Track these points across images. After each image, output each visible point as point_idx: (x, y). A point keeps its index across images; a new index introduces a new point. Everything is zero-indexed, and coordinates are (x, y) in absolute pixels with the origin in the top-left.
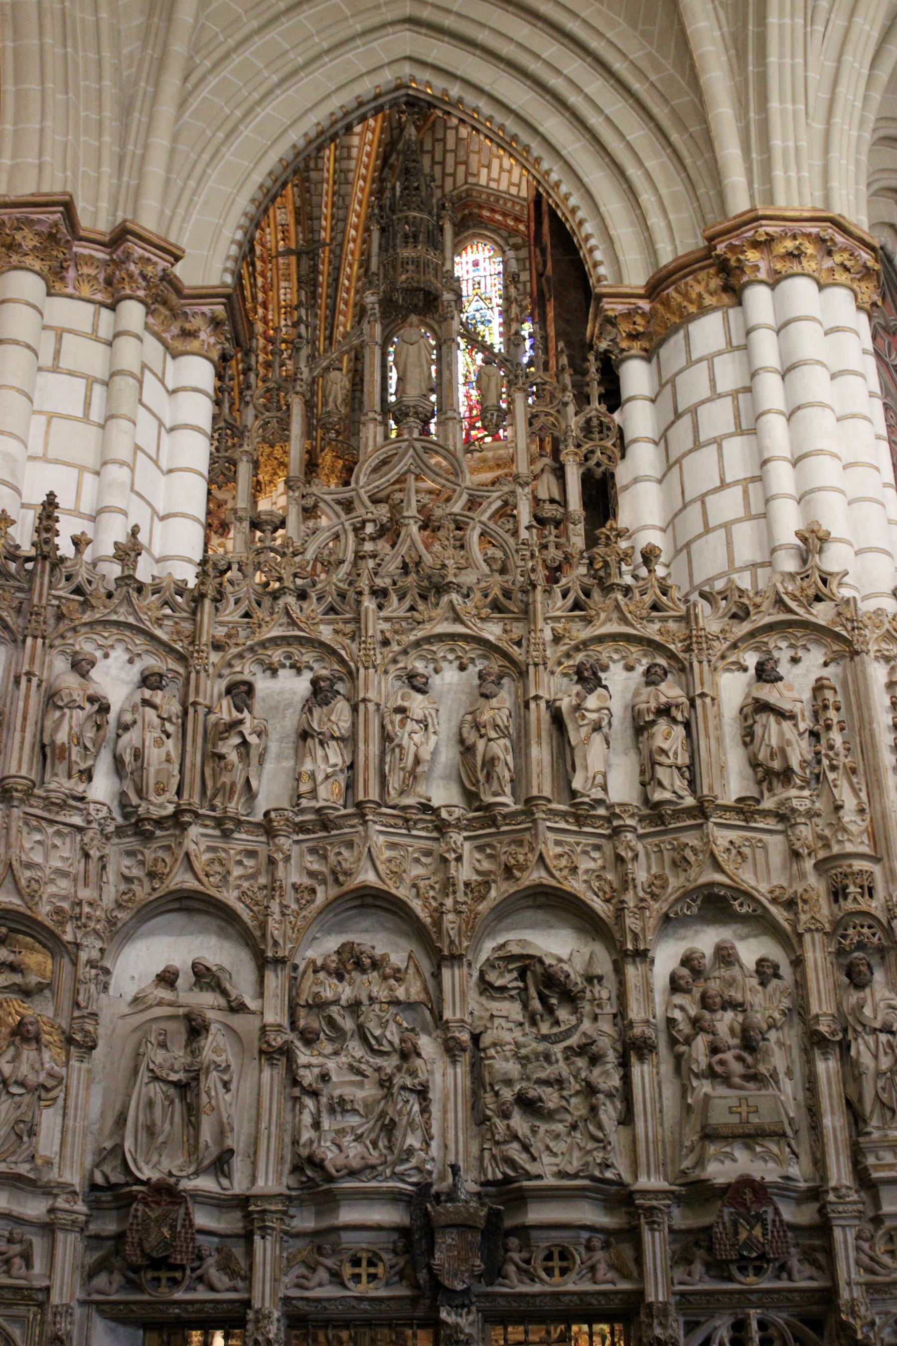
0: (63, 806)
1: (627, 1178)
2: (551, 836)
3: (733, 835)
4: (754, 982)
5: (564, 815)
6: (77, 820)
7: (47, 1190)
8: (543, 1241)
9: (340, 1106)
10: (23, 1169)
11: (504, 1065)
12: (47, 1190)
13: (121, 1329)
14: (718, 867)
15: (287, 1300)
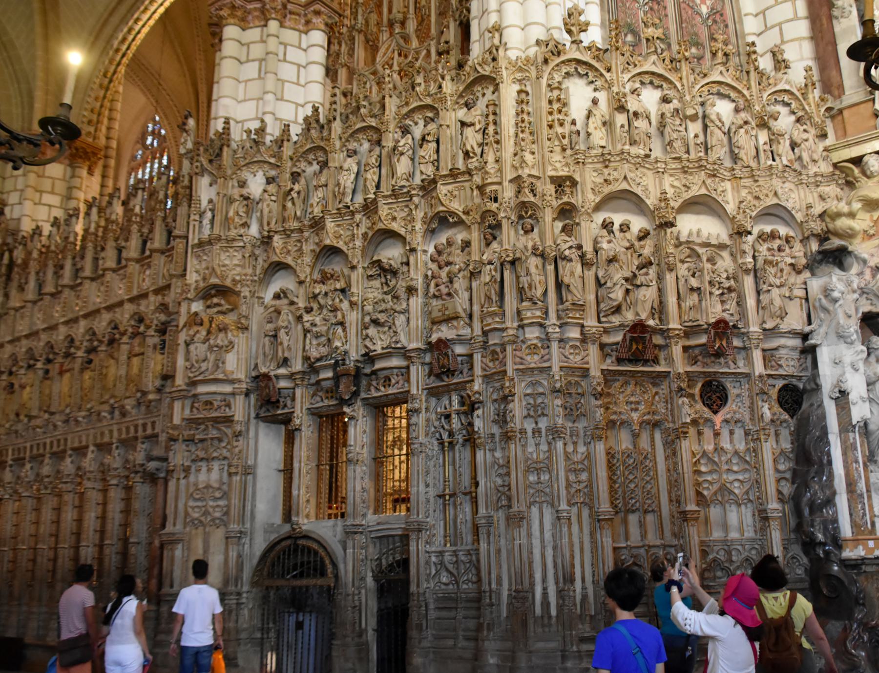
0: (234, 240)
1: (406, 345)
2: (386, 207)
3: (450, 187)
4: (459, 251)
5: (389, 196)
6: (241, 244)
7: (232, 382)
8: (382, 374)
9: (317, 336)
10: (221, 376)
11: (369, 308)
12: (232, 382)
13: (273, 426)
14: (443, 205)
15: (308, 409)
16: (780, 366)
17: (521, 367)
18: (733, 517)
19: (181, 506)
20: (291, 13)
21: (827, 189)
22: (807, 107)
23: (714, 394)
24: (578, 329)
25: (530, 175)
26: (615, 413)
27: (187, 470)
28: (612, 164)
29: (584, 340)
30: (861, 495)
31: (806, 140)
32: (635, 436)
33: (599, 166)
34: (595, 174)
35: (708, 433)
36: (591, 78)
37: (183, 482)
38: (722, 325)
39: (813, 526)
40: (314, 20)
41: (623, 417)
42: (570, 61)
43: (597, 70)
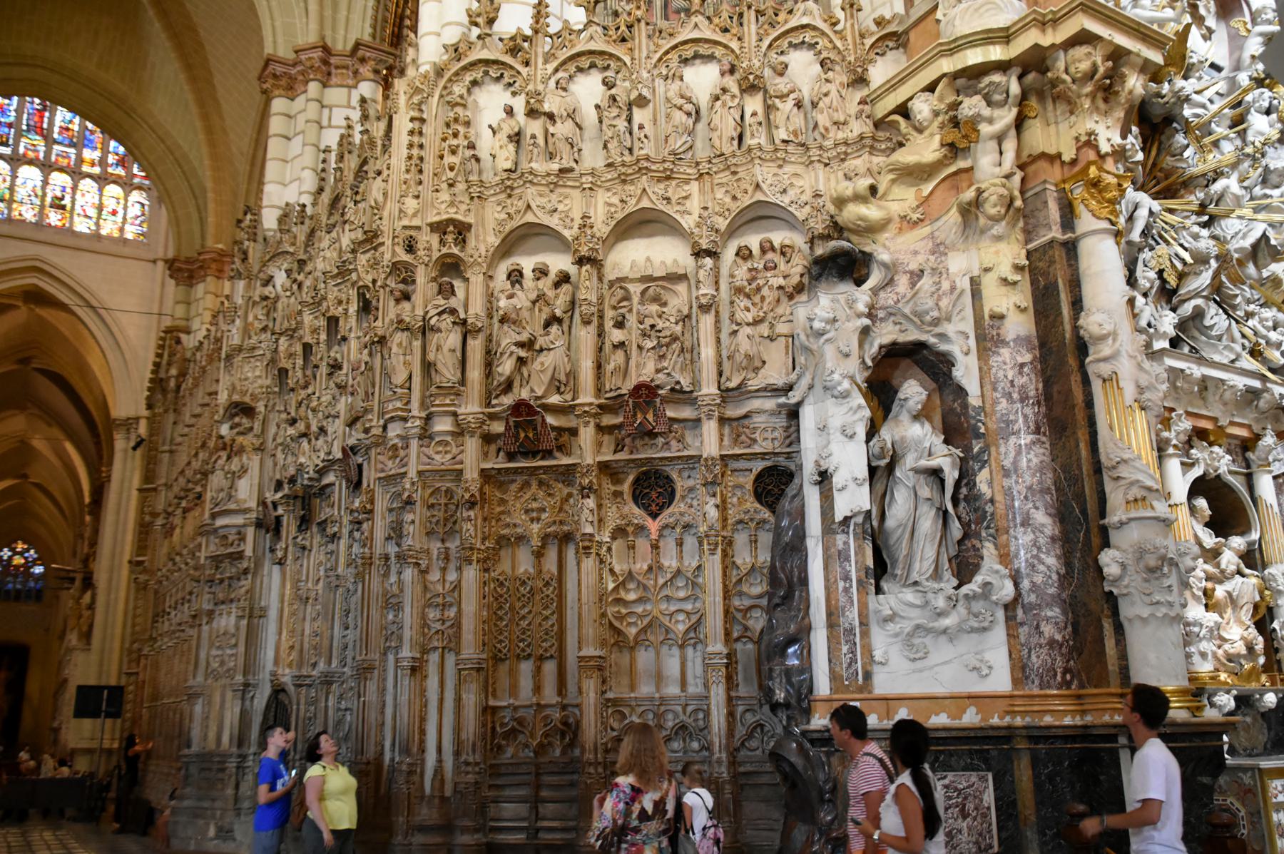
16: (755, 441)
17: (382, 475)
18: (672, 665)
19: (203, 655)
20: (337, 67)
21: (858, 162)
22: (839, 44)
23: (653, 489)
24: (449, 420)
25: (405, 227)
26: (508, 525)
27: (210, 614)
28: (516, 191)
29: (460, 432)
30: (850, 631)
31: (826, 95)
32: (539, 555)
33: (503, 196)
34: (499, 208)
35: (643, 545)
36: (506, 80)
37: (205, 628)
38: (644, 391)
39: (771, 678)
40: (361, 70)
41: (519, 530)
42: (473, 64)
43: (512, 67)
